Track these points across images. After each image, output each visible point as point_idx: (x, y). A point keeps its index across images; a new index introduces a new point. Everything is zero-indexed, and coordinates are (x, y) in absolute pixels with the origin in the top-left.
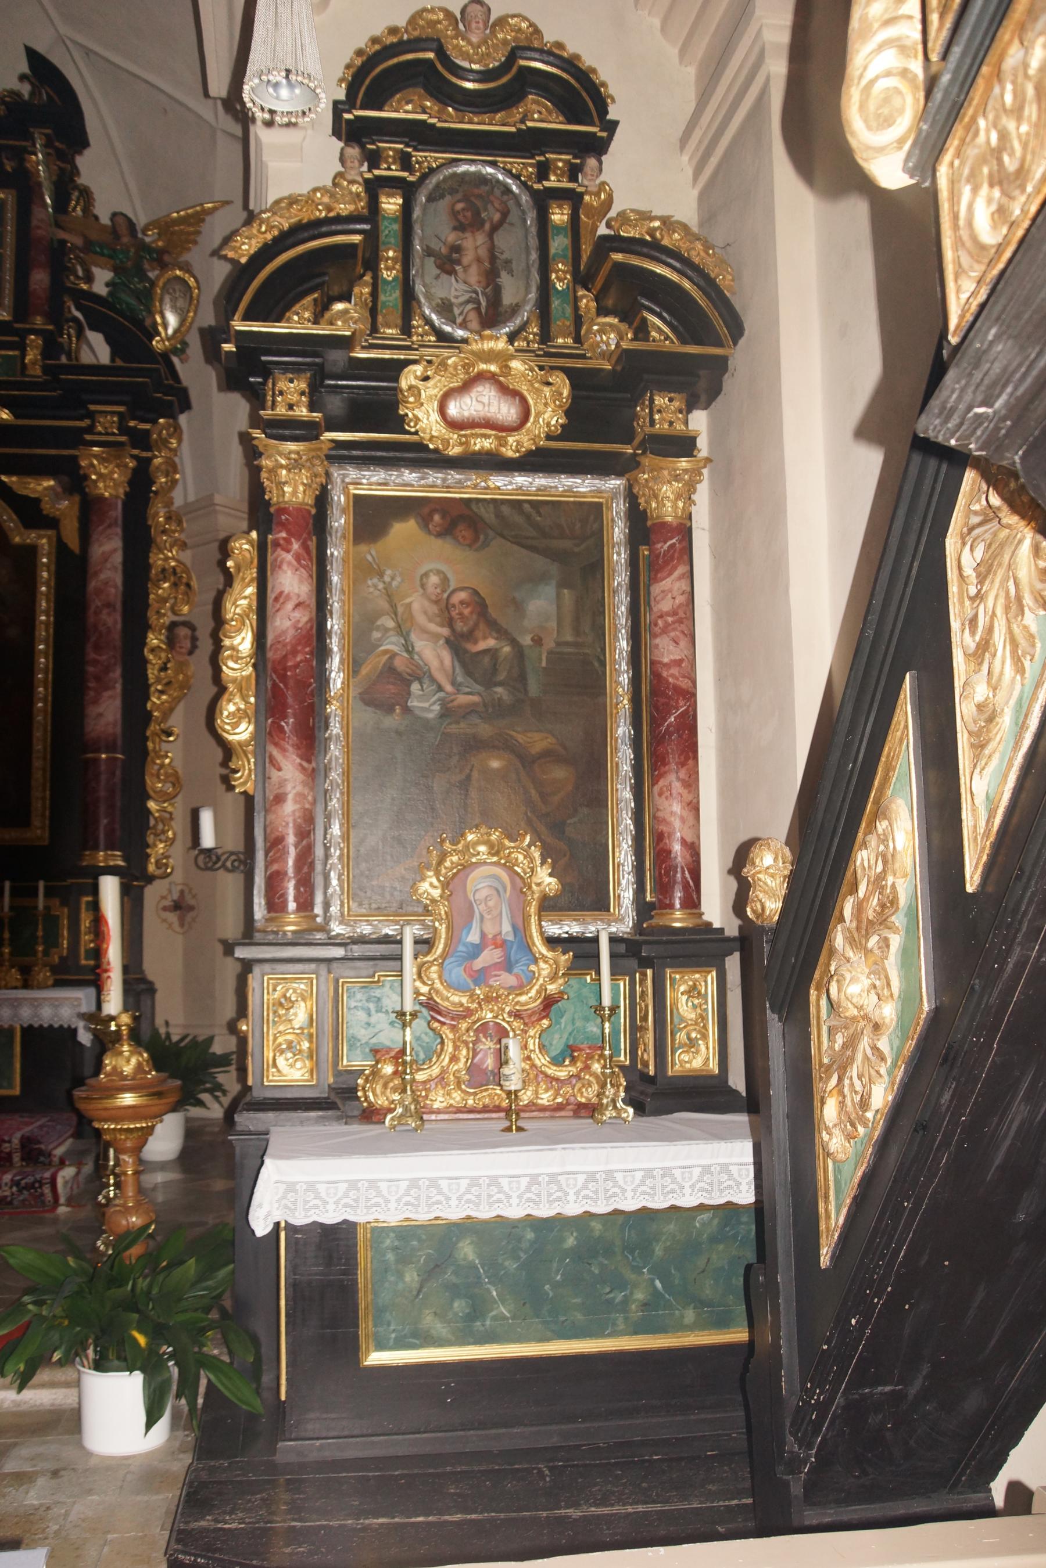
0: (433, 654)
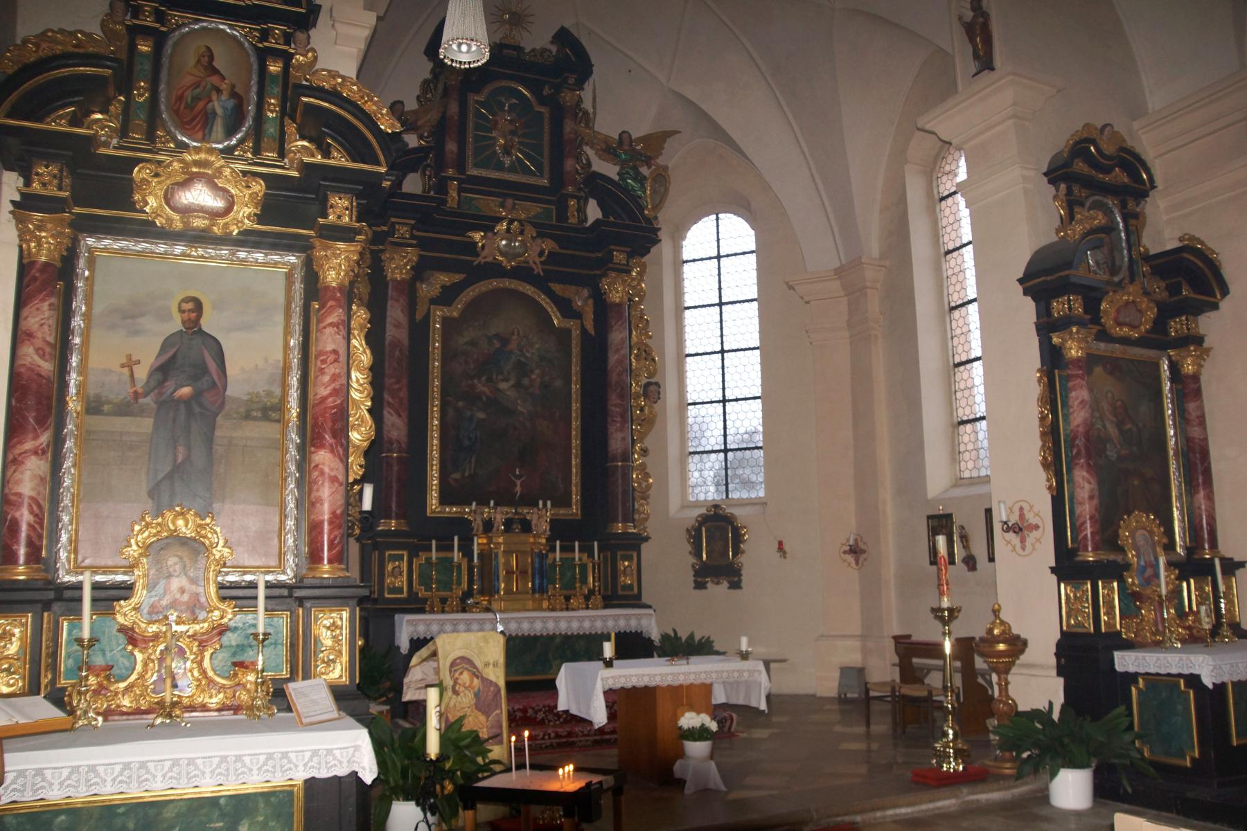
0: (1113, 431)
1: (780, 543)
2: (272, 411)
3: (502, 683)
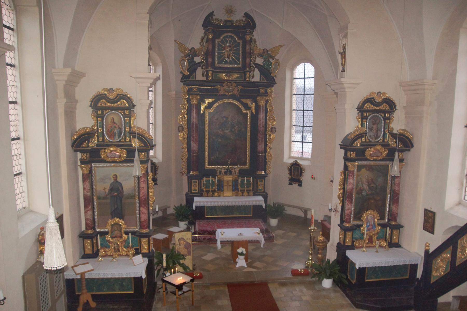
0: (366, 187)
1: (312, 176)
2: (133, 197)
3: (191, 243)
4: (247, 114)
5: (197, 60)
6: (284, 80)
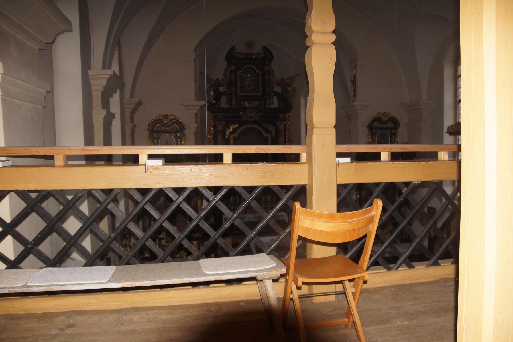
4: (268, 137)
5: (221, 89)
6: (299, 106)
